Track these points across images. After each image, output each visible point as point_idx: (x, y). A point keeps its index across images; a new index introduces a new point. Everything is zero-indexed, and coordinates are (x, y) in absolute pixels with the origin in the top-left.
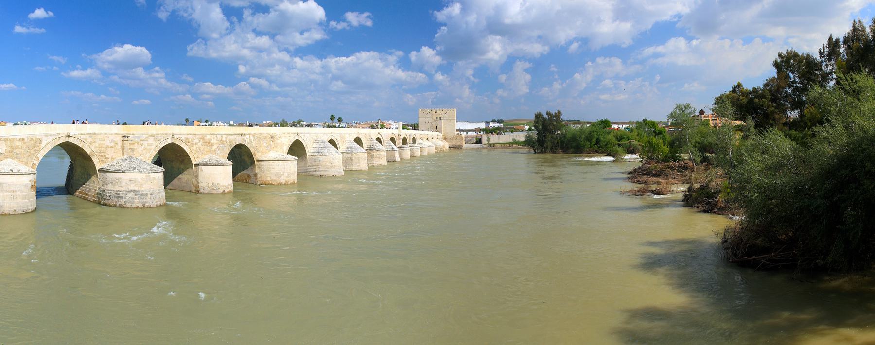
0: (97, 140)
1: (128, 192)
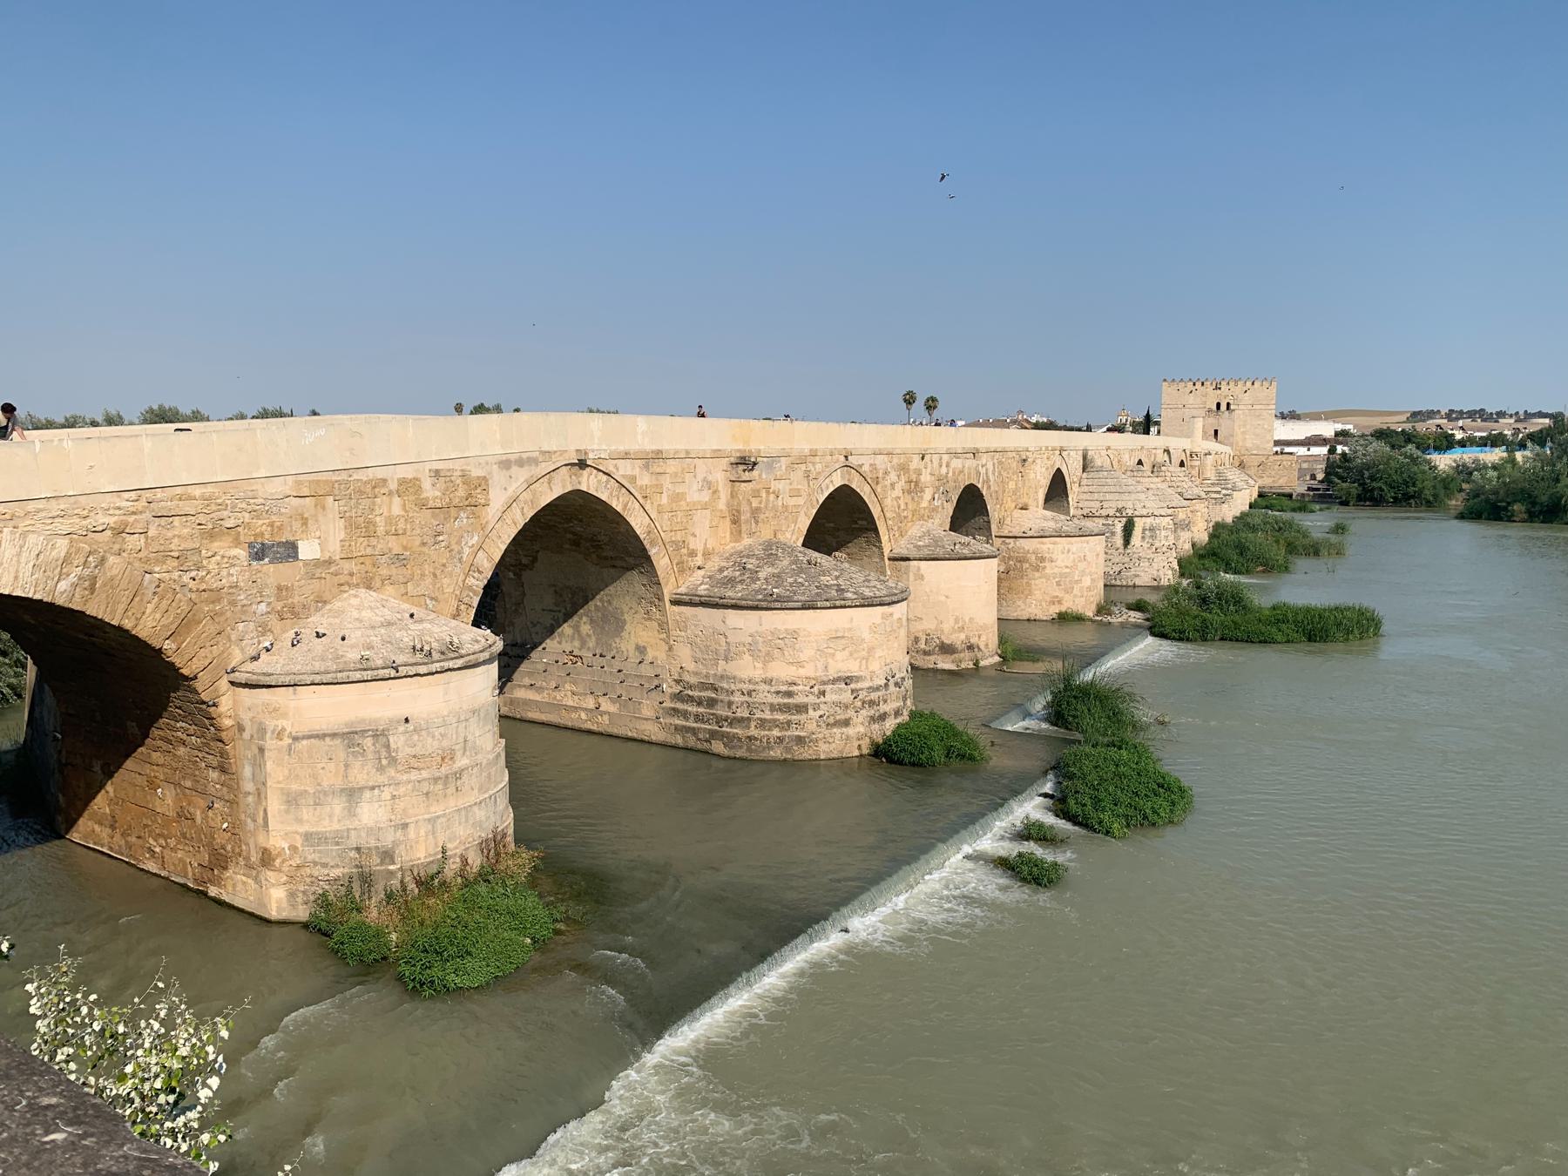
0: (666, 482)
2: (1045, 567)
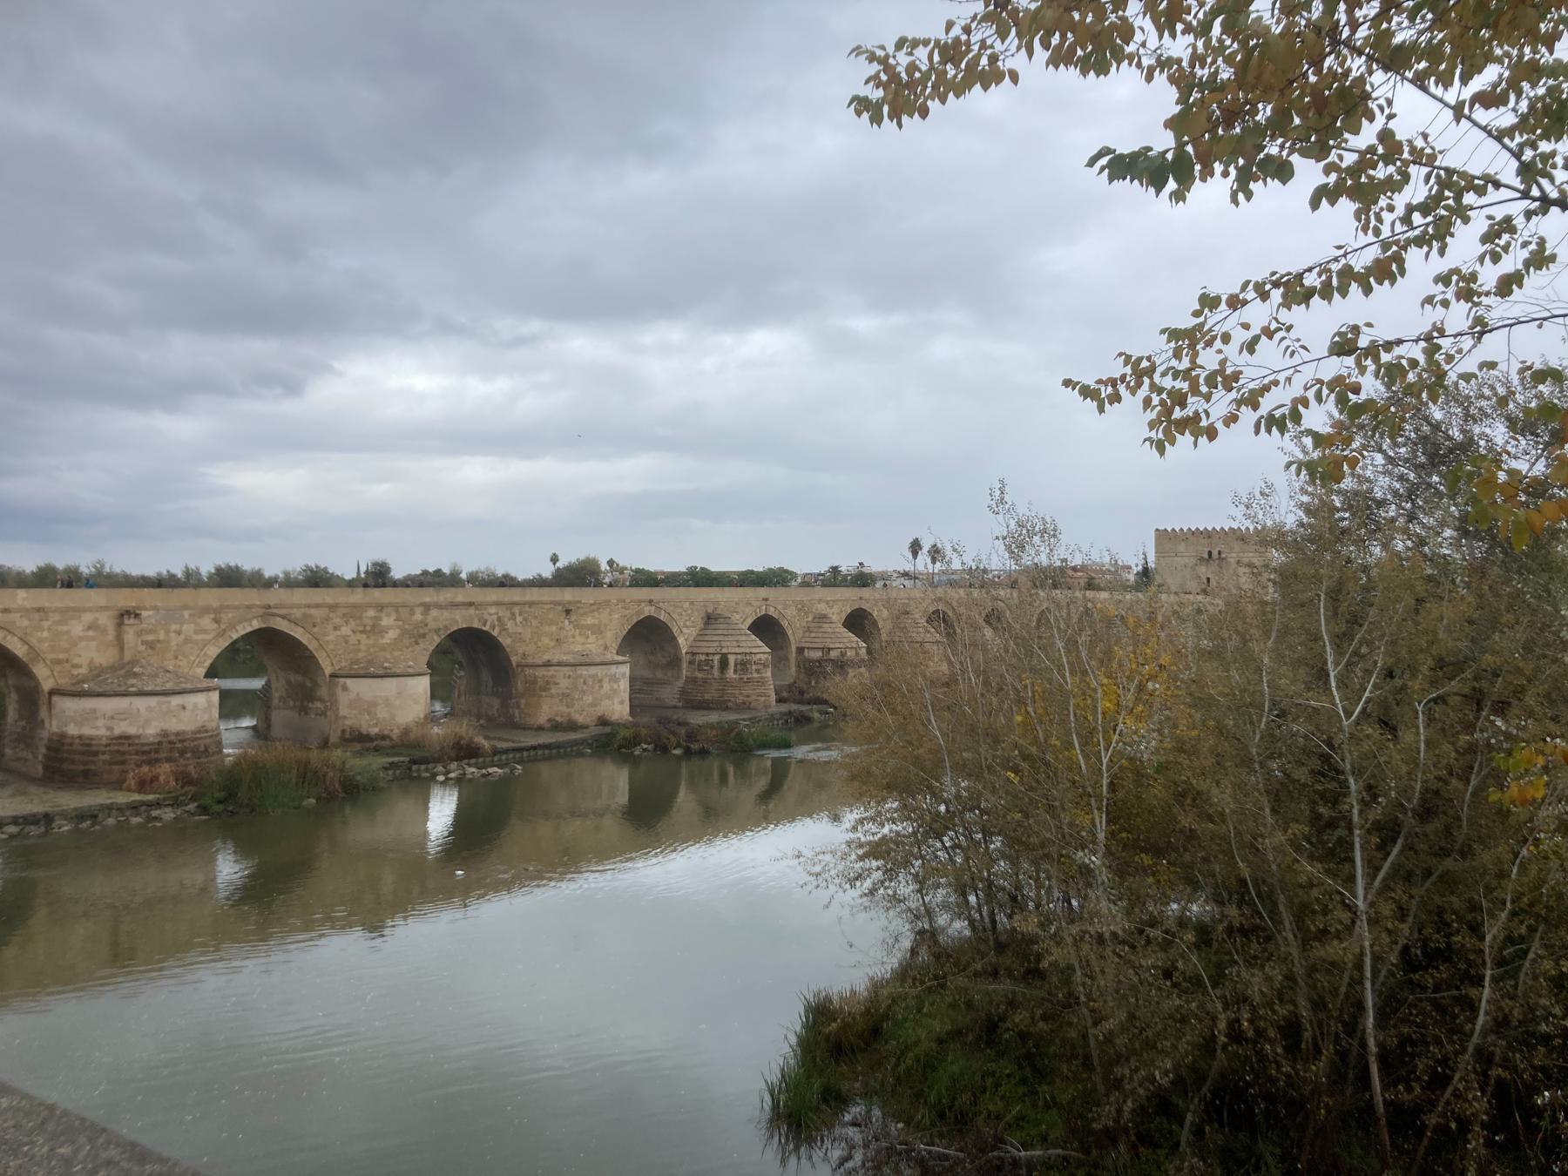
2: (550, 689)
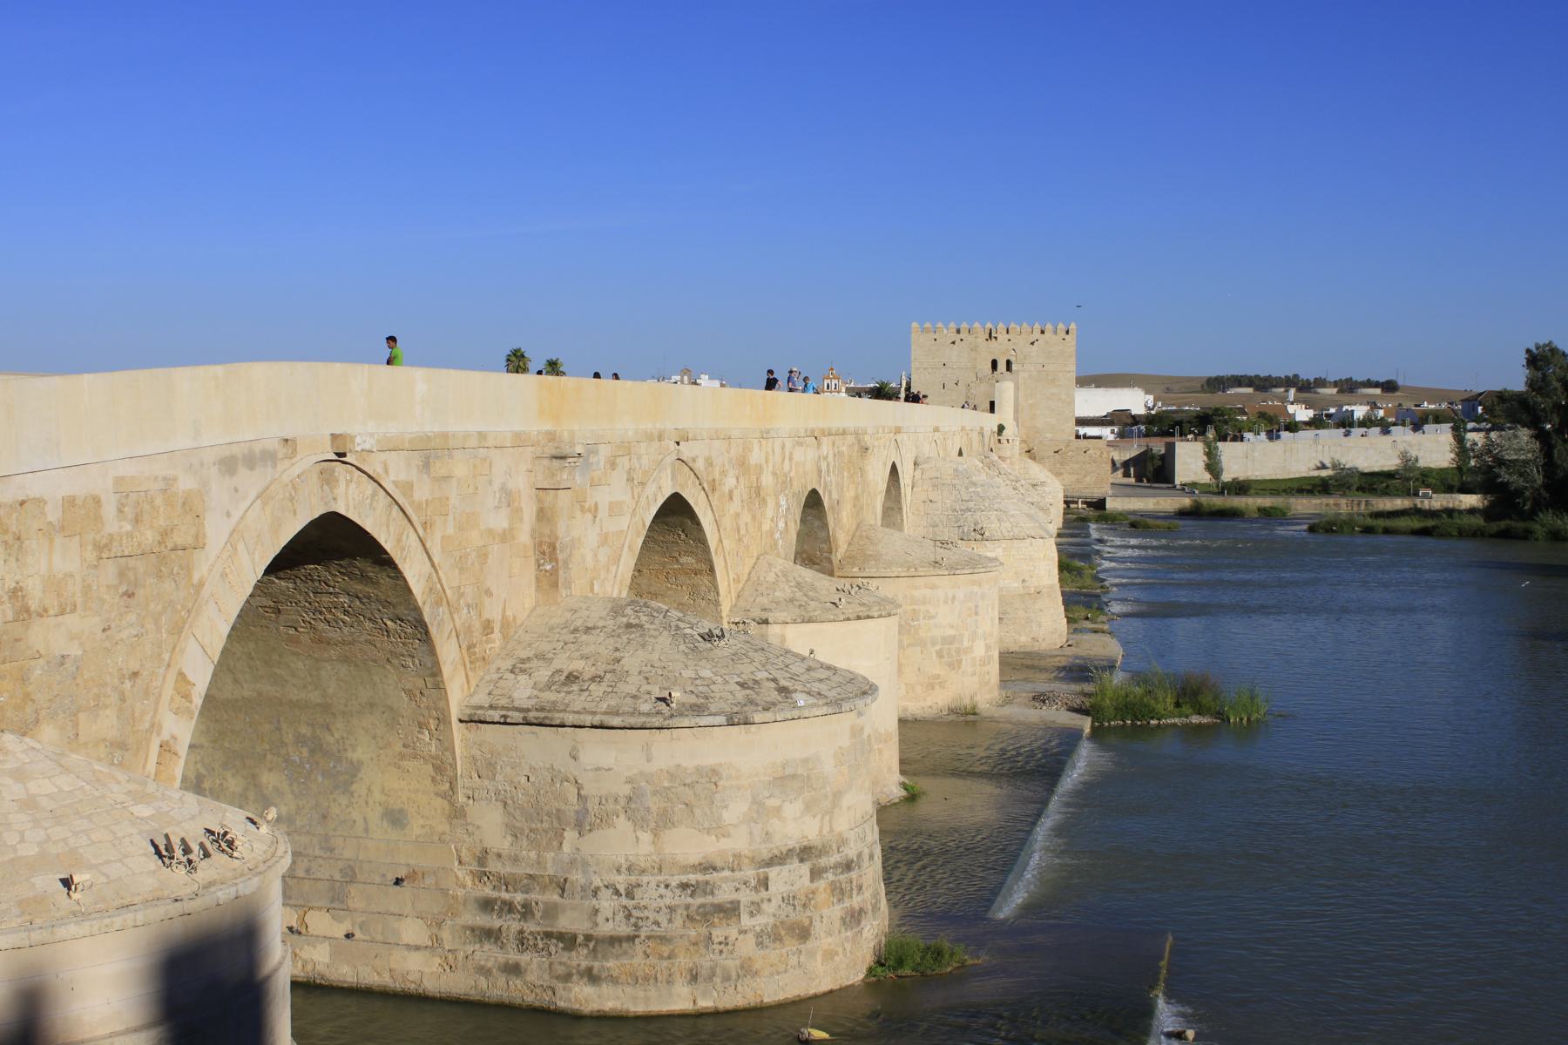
1: (771, 862)
